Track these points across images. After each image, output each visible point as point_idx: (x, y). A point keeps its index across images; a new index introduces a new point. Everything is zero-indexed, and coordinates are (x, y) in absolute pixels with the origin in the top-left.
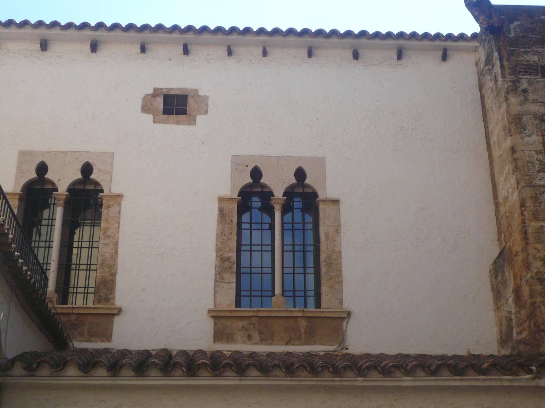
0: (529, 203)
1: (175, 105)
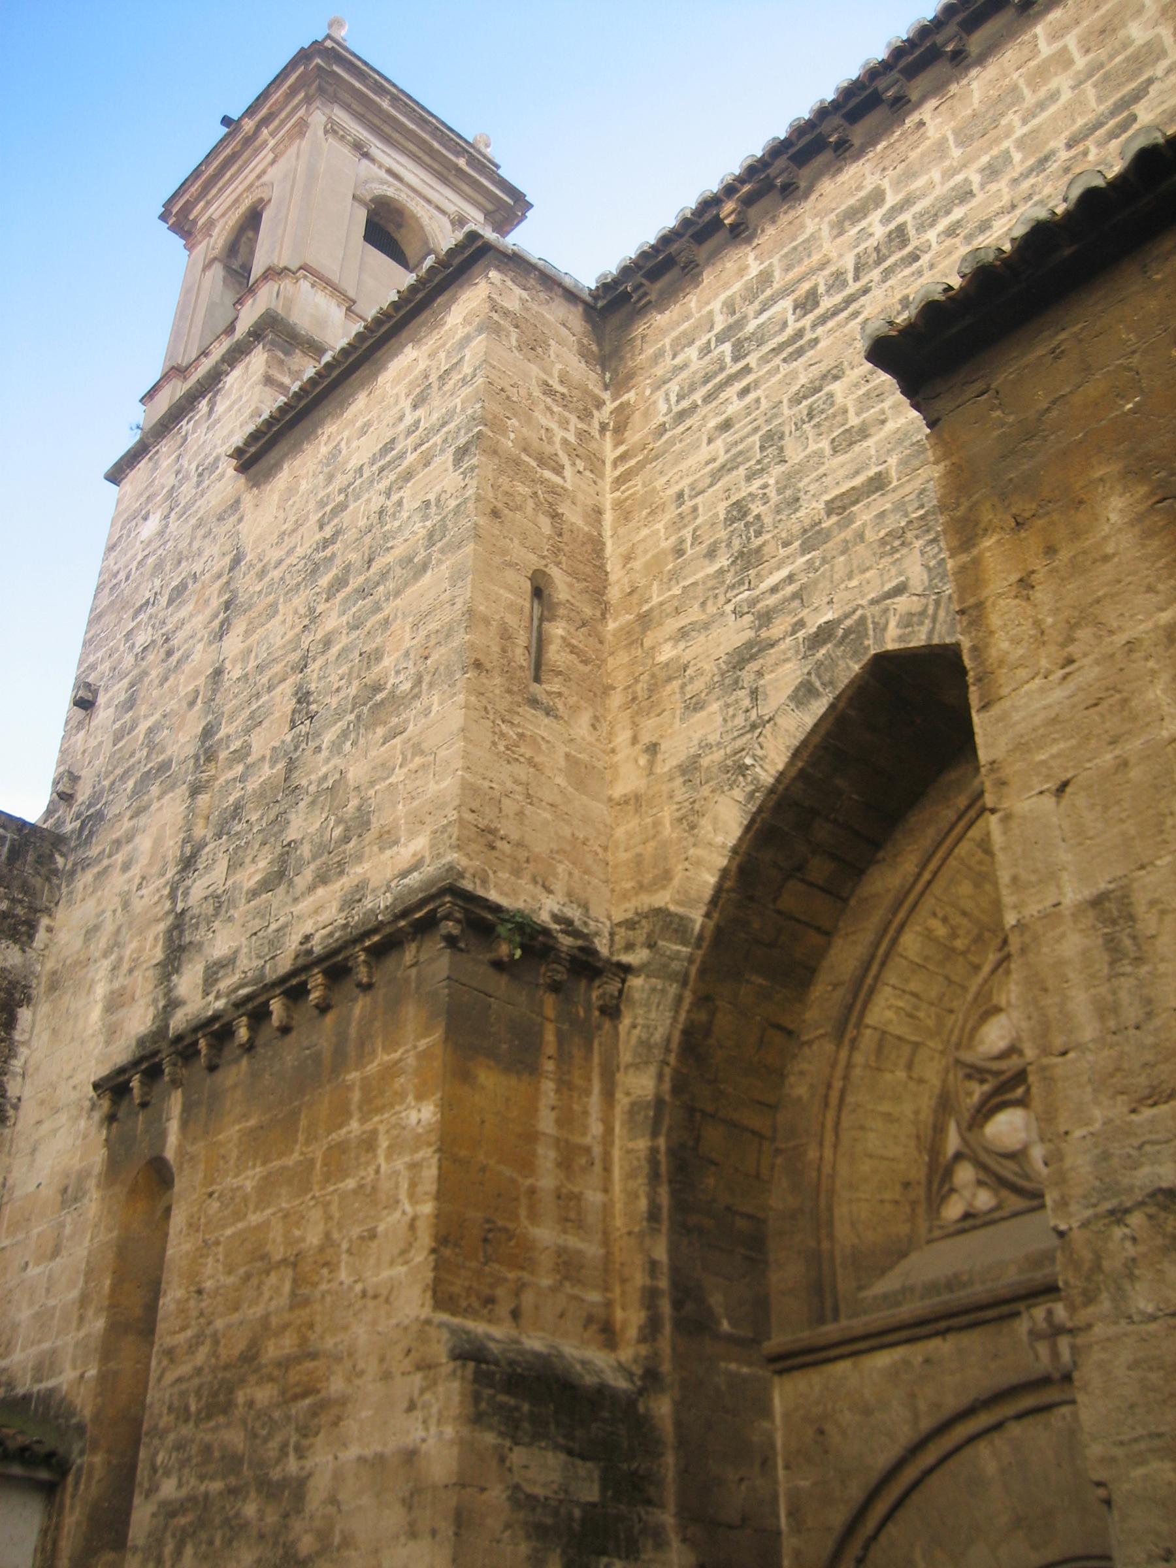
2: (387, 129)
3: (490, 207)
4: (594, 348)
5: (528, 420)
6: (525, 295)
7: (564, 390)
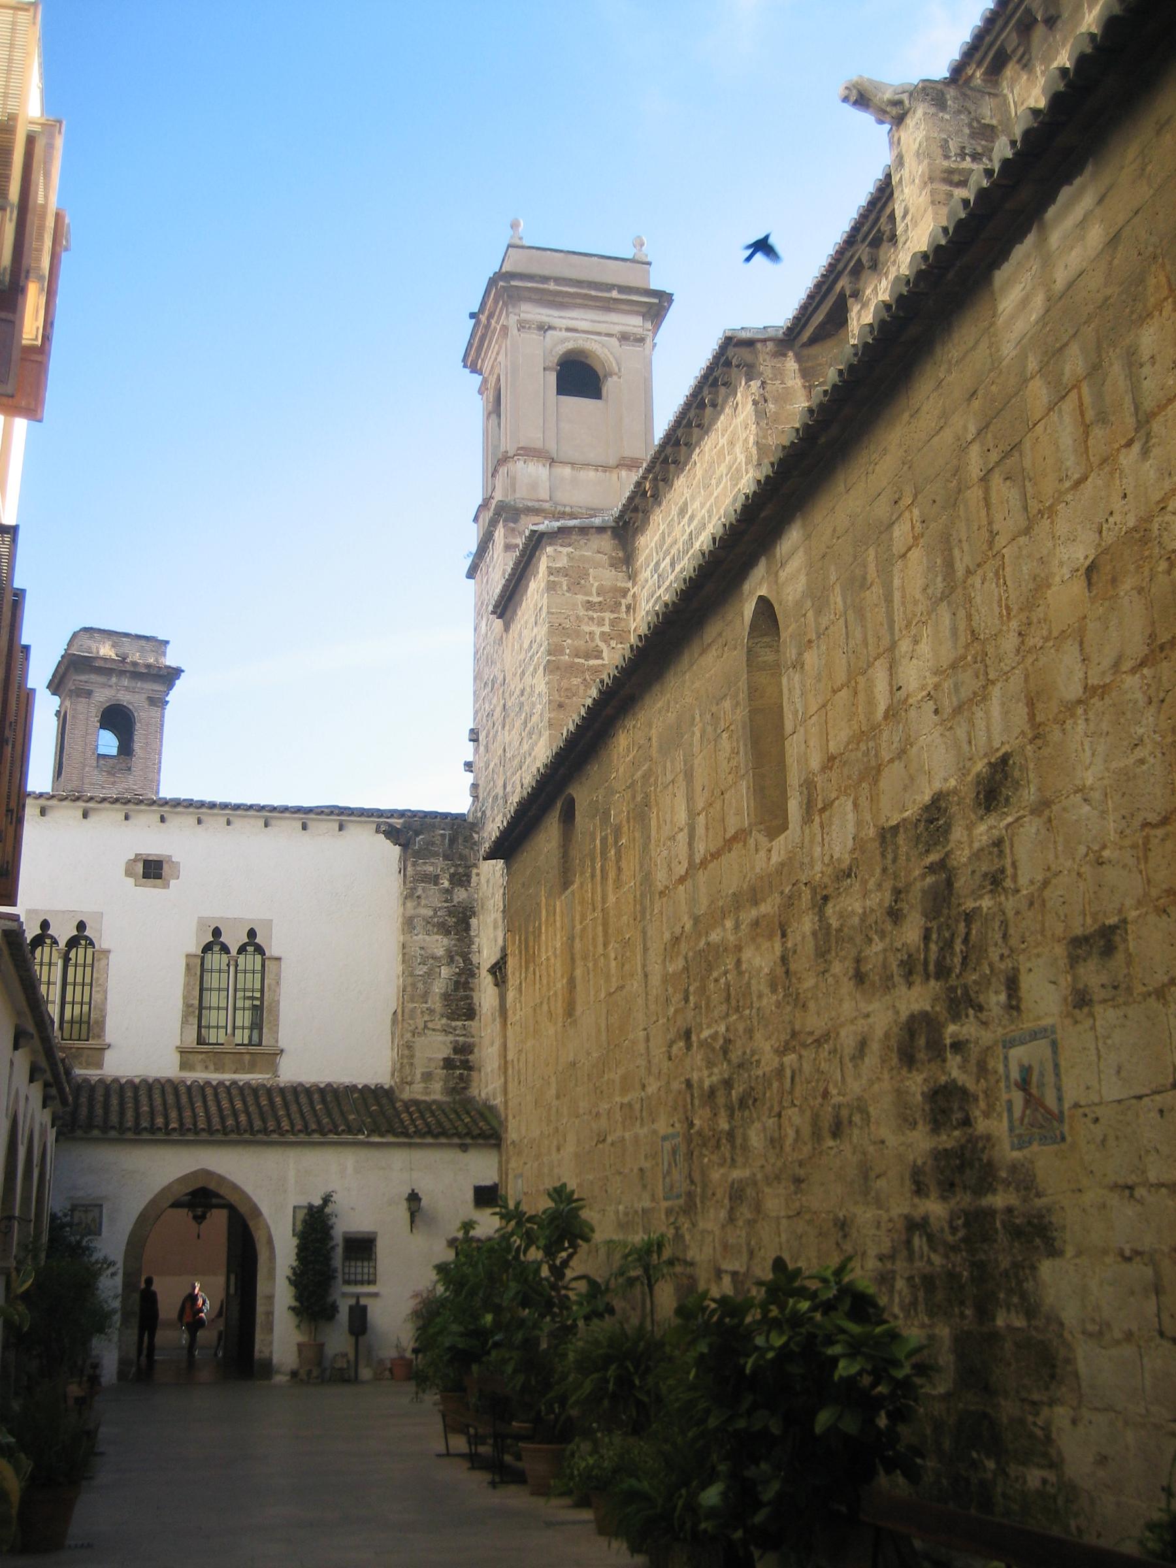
0: (409, 989)
1: (152, 870)
2: (560, 299)
3: (644, 310)
4: (621, 554)
5: (577, 634)
6: (570, 549)
7: (601, 599)
